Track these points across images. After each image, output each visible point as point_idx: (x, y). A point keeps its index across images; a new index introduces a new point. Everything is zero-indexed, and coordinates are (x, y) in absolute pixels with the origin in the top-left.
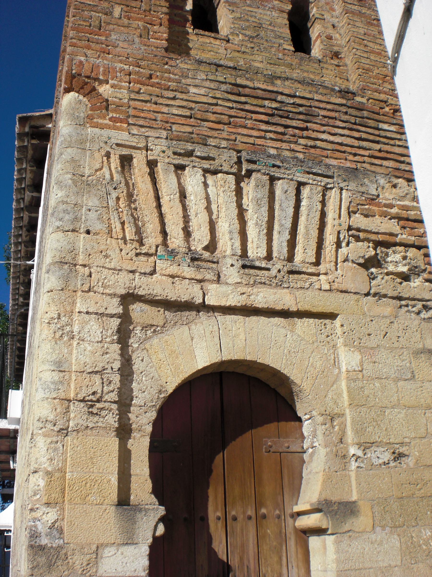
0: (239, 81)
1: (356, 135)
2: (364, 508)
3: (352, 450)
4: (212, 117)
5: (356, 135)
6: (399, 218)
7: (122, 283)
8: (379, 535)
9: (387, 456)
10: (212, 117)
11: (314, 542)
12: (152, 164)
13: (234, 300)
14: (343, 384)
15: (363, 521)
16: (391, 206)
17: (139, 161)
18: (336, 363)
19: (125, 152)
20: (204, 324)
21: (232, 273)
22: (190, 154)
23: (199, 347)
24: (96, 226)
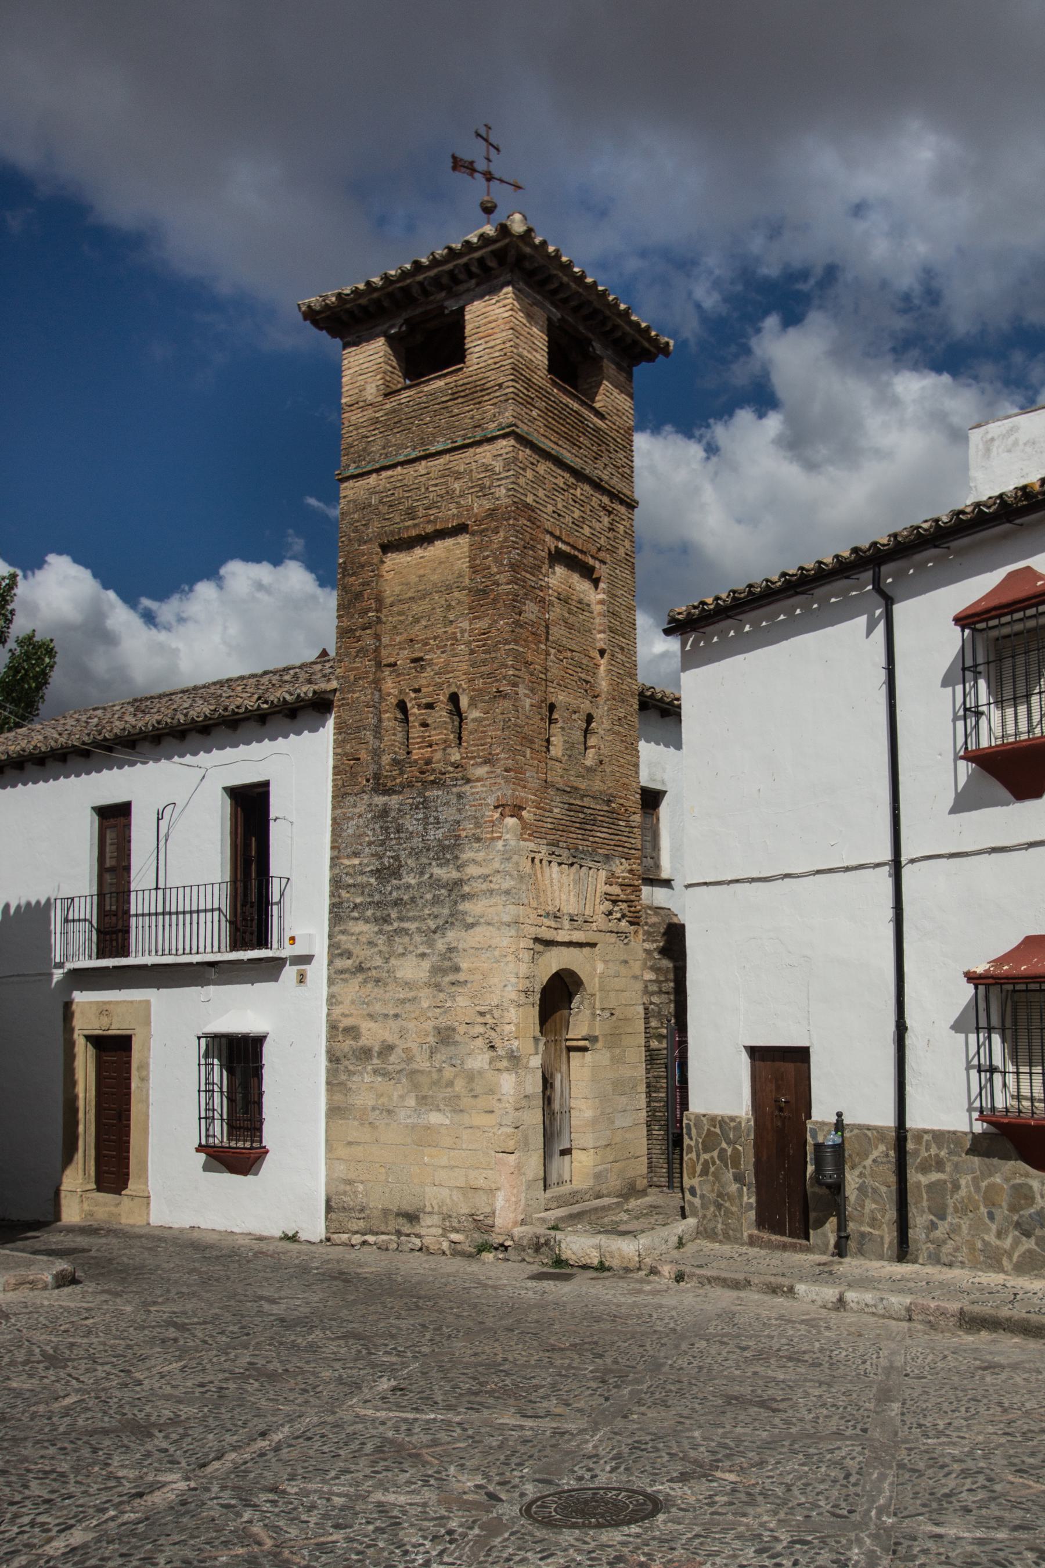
0: (572, 801)
1: (610, 831)
2: (600, 1038)
3: (598, 1012)
4: (561, 828)
5: (610, 831)
6: (621, 885)
7: (533, 931)
8: (604, 1051)
9: (608, 1015)
10: (561, 828)
11: (572, 1054)
12: (541, 861)
13: (567, 939)
14: (597, 980)
15: (599, 1045)
16: (618, 878)
17: (537, 861)
18: (595, 970)
19: (533, 855)
20: (555, 951)
21: (566, 923)
22: (553, 853)
23: (555, 961)
24: (526, 902)
